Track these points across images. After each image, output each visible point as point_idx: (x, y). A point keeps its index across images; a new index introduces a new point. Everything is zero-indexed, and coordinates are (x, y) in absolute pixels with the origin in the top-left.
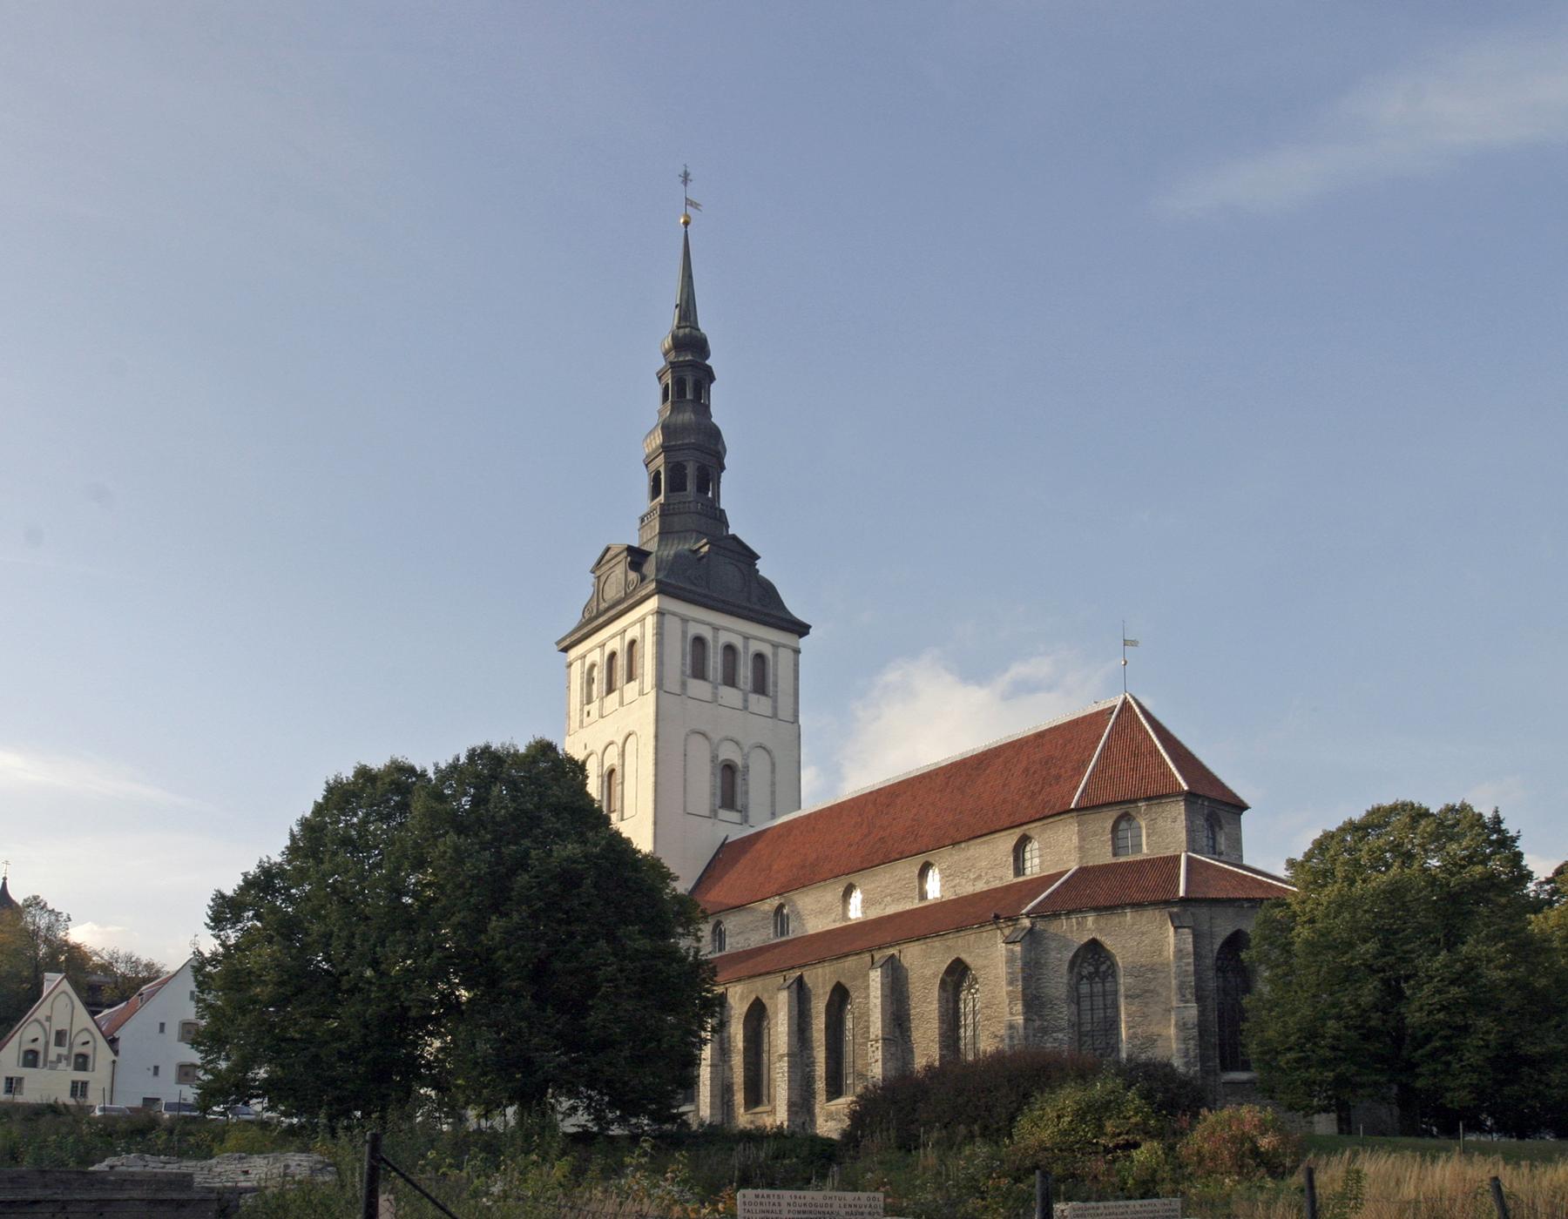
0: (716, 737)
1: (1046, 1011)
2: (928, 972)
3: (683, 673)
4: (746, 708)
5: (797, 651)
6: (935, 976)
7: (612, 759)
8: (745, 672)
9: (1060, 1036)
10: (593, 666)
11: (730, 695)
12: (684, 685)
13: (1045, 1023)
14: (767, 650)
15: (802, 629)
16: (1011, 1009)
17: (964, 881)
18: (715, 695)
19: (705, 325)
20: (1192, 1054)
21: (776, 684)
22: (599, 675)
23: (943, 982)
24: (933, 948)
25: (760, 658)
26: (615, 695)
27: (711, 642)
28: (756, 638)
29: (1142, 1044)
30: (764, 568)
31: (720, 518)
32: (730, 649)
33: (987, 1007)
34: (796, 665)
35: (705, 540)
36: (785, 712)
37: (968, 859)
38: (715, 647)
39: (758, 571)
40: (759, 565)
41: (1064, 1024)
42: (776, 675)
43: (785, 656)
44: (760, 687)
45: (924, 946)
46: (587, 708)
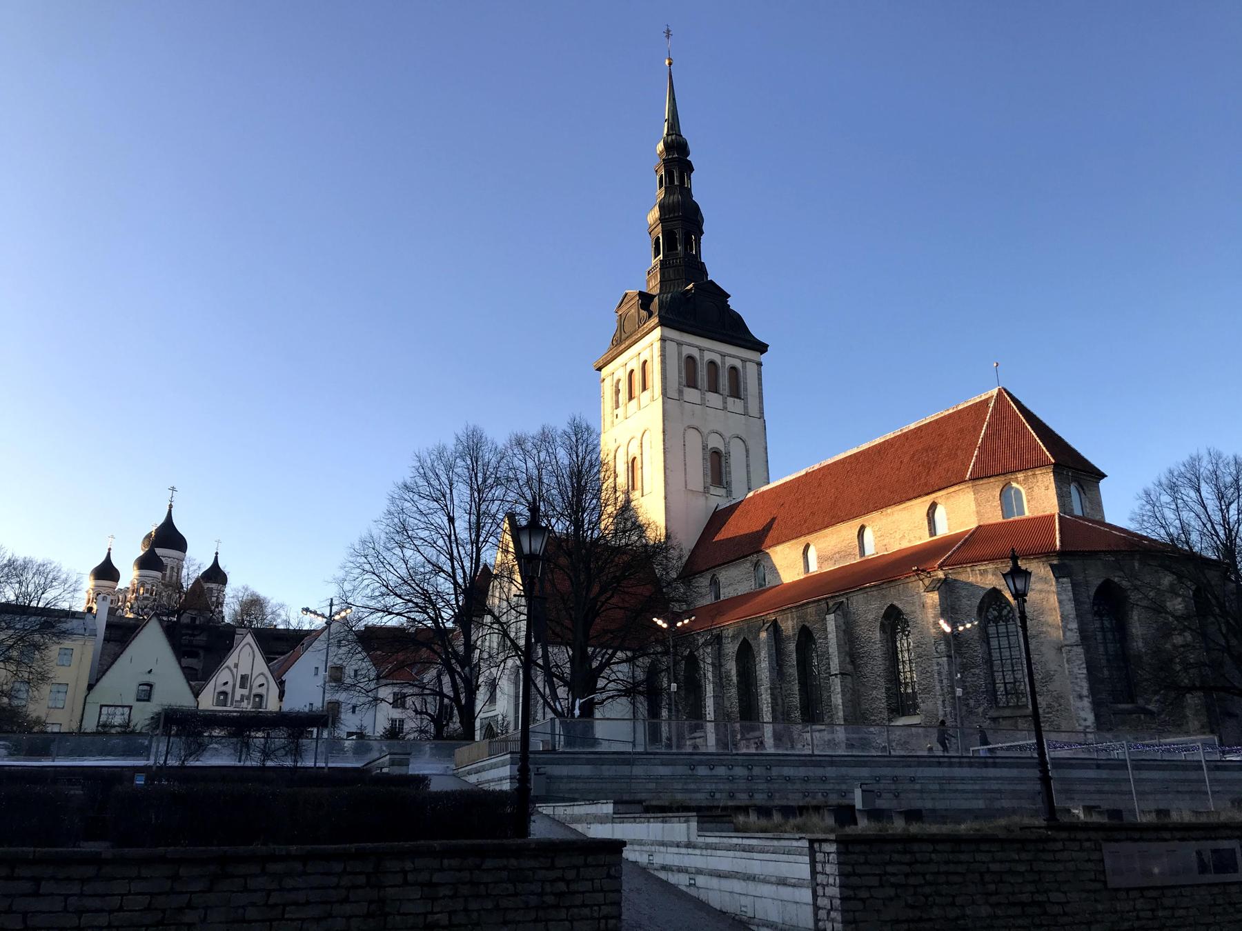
0: (705, 431)
1: (964, 649)
2: (871, 617)
3: (680, 384)
4: (725, 408)
5: (760, 364)
6: (876, 620)
7: (634, 451)
8: (724, 381)
9: (977, 671)
10: (619, 381)
11: (713, 399)
12: (681, 392)
13: (965, 660)
14: (738, 364)
15: (762, 348)
17: (893, 540)
18: (703, 399)
21: (746, 390)
22: (624, 387)
23: (882, 625)
24: (873, 596)
25: (733, 369)
26: (634, 402)
27: (698, 359)
28: (730, 356)
30: (733, 304)
31: (701, 269)
32: (712, 363)
33: (918, 646)
34: (760, 374)
35: (541, 554)
36: (753, 410)
37: (894, 522)
38: (702, 364)
39: (729, 306)
40: (730, 301)
41: (979, 661)
42: (745, 383)
43: (752, 368)
44: (736, 391)
46: (616, 412)
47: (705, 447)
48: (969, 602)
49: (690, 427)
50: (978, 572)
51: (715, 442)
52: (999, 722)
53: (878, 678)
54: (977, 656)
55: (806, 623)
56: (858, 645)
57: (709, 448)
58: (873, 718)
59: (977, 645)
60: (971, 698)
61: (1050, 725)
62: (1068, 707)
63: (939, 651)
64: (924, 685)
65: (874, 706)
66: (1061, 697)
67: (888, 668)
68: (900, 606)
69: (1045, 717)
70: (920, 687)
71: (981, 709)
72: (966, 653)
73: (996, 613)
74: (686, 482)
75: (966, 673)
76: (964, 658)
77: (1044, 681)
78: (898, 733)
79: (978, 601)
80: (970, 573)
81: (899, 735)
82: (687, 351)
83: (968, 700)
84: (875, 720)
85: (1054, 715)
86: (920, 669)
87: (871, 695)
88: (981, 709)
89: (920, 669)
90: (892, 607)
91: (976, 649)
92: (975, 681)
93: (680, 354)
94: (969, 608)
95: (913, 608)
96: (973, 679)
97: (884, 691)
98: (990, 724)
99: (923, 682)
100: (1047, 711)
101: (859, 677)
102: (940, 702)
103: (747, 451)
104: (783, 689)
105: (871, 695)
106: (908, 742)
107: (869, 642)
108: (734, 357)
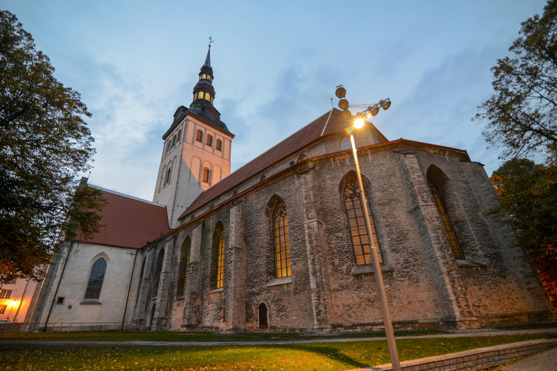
0: (203, 160)
1: (329, 218)
2: (259, 206)
4: (213, 153)
5: (231, 141)
7: (170, 166)
9: (340, 234)
13: (329, 226)
14: (222, 139)
15: (232, 136)
16: (307, 215)
19: (213, 65)
20: (442, 241)
21: (224, 149)
23: (267, 211)
29: (397, 238)
30: (222, 119)
33: (292, 221)
36: (226, 156)
42: (224, 146)
44: (219, 148)
45: (257, 193)
47: (201, 166)
48: (332, 183)
49: (195, 156)
50: (338, 161)
51: (206, 165)
52: (362, 278)
53: (261, 249)
54: (340, 223)
55: (221, 220)
56: (250, 227)
57: (204, 166)
58: (255, 280)
59: (339, 213)
60: (336, 257)
61: (409, 279)
62: (424, 262)
63: (309, 216)
64: (295, 250)
65: (257, 271)
66: (416, 253)
67: (269, 241)
68: (280, 195)
69: (403, 272)
70: (293, 252)
71: (344, 267)
72: (330, 221)
73: (351, 192)
74: (190, 178)
75: (331, 236)
76: (329, 224)
77: (398, 239)
78: (273, 292)
79: (339, 181)
80: (332, 162)
81: (274, 293)
82: (198, 128)
83: (333, 259)
84: (257, 282)
85: (412, 269)
86: (293, 238)
87: (255, 262)
88: (344, 267)
89: (293, 238)
90: (275, 197)
91: (338, 217)
92: (339, 243)
93: (195, 128)
94: (332, 187)
95: (289, 194)
96: (338, 241)
97: (264, 258)
98: (354, 280)
99: (295, 248)
100: (404, 266)
101: (248, 250)
102: (310, 261)
103: (221, 171)
104: (203, 264)
105: (255, 262)
106: (281, 300)
107: (257, 224)
108: (221, 136)
